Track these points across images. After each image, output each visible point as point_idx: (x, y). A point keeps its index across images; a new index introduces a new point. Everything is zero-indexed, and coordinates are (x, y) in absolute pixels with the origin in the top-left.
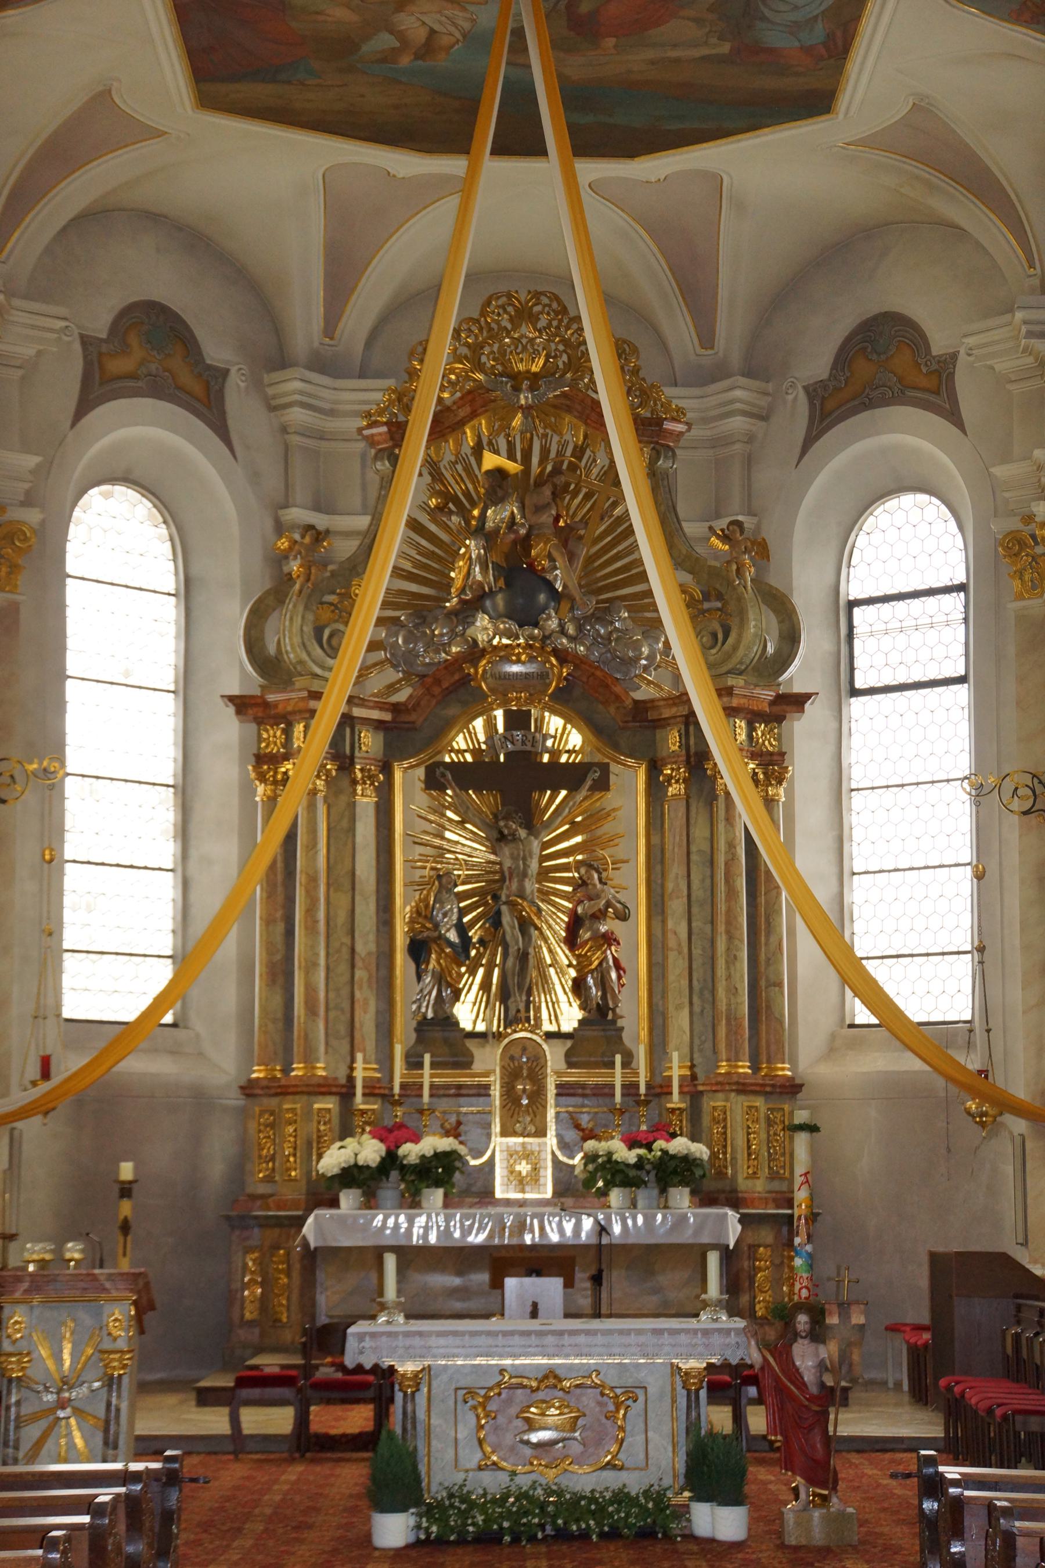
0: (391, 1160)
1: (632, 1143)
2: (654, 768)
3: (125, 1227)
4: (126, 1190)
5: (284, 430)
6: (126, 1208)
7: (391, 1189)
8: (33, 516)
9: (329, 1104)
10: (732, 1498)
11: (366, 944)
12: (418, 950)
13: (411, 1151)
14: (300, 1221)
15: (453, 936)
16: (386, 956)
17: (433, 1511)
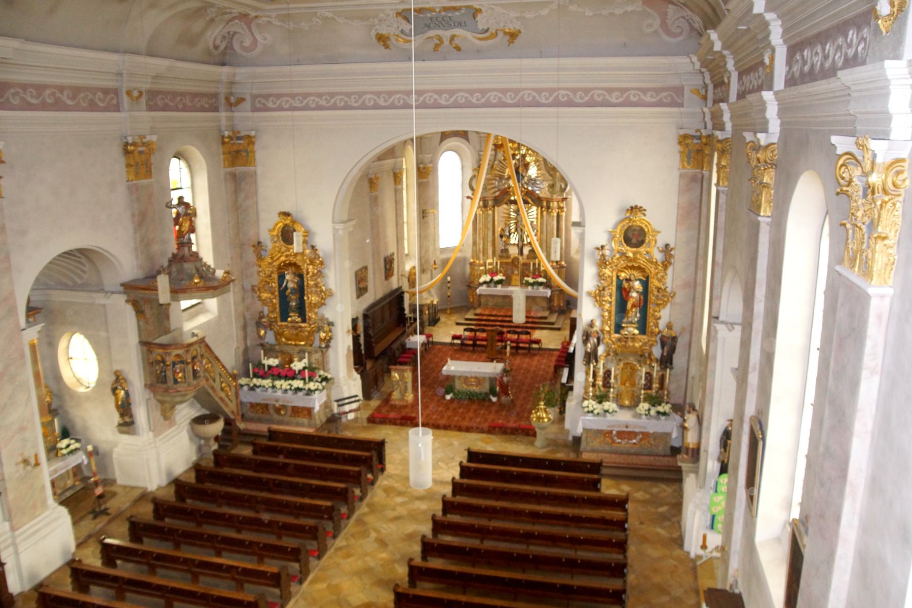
0: (492, 280)
1: (533, 278)
2: (542, 208)
3: (449, 288)
4: (449, 282)
5: (480, 137)
6: (449, 285)
7: (492, 284)
8: (431, 165)
9: (482, 268)
10: (494, 396)
11: (490, 239)
12: (501, 236)
13: (496, 278)
14: (477, 288)
15: (508, 234)
16: (494, 240)
17: (455, 394)
